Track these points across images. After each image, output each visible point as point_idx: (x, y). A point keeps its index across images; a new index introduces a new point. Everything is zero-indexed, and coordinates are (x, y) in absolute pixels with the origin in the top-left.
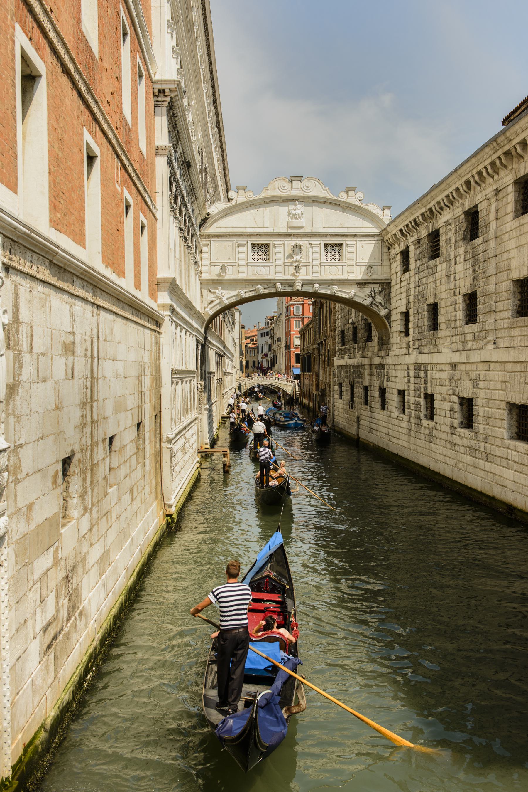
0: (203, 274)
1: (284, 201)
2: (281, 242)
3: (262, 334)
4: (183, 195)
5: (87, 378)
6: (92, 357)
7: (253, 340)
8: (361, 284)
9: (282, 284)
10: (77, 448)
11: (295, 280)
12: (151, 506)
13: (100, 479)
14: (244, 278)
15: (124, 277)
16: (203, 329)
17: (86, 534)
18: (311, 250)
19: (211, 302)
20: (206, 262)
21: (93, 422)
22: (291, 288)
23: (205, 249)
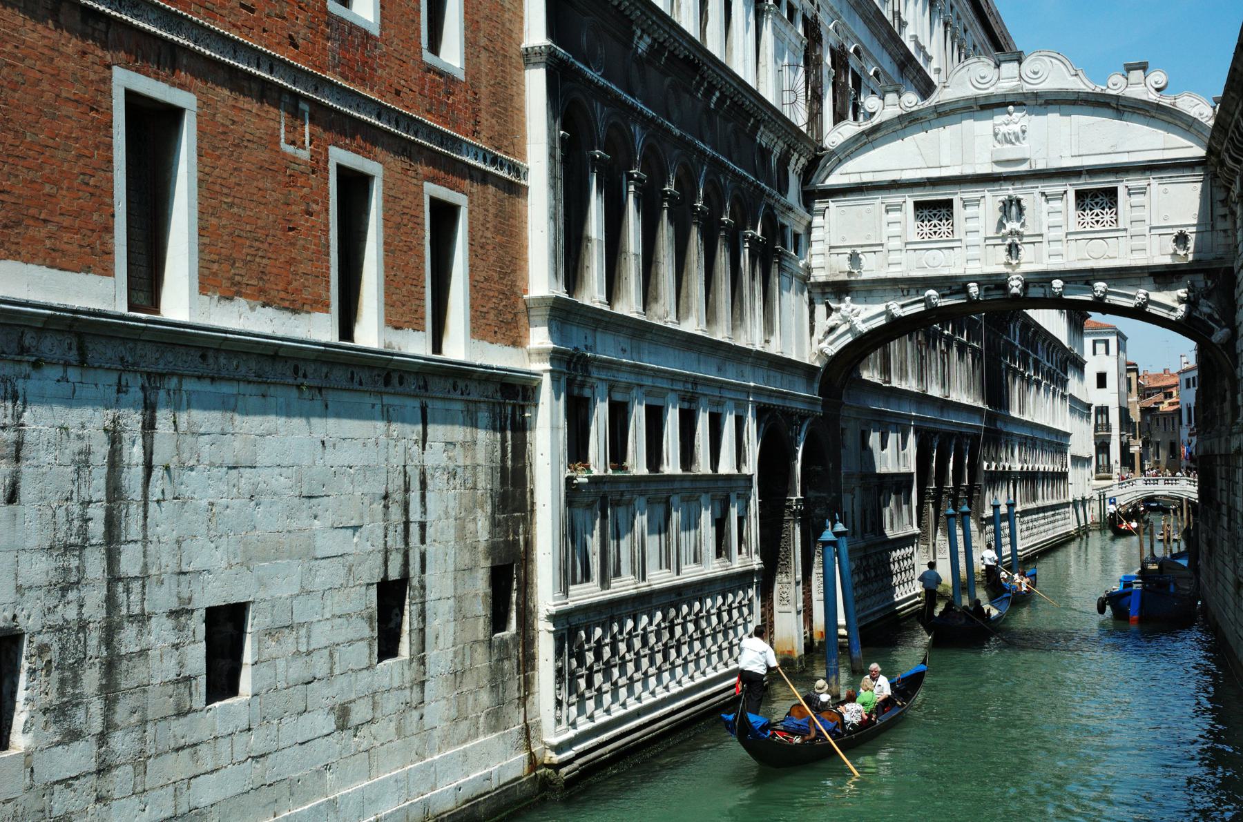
0: (815, 273)
1: (984, 108)
2: (978, 195)
3: (1188, 380)
4: (661, 126)
5: (86, 504)
6: (115, 462)
7: (1169, 395)
8: (1163, 276)
9: (979, 286)
10: (29, 623)
11: (1008, 275)
12: (465, 741)
13: (156, 681)
14: (899, 276)
15: (327, 312)
16: (816, 386)
17: (77, 778)
18: (1044, 204)
19: (832, 329)
20: (816, 248)
21: (113, 578)
22: (1001, 292)
23: (817, 220)
